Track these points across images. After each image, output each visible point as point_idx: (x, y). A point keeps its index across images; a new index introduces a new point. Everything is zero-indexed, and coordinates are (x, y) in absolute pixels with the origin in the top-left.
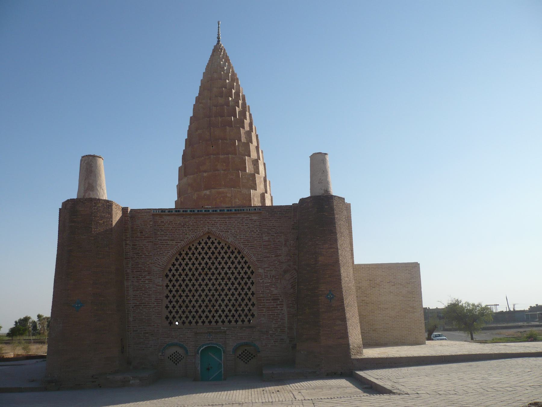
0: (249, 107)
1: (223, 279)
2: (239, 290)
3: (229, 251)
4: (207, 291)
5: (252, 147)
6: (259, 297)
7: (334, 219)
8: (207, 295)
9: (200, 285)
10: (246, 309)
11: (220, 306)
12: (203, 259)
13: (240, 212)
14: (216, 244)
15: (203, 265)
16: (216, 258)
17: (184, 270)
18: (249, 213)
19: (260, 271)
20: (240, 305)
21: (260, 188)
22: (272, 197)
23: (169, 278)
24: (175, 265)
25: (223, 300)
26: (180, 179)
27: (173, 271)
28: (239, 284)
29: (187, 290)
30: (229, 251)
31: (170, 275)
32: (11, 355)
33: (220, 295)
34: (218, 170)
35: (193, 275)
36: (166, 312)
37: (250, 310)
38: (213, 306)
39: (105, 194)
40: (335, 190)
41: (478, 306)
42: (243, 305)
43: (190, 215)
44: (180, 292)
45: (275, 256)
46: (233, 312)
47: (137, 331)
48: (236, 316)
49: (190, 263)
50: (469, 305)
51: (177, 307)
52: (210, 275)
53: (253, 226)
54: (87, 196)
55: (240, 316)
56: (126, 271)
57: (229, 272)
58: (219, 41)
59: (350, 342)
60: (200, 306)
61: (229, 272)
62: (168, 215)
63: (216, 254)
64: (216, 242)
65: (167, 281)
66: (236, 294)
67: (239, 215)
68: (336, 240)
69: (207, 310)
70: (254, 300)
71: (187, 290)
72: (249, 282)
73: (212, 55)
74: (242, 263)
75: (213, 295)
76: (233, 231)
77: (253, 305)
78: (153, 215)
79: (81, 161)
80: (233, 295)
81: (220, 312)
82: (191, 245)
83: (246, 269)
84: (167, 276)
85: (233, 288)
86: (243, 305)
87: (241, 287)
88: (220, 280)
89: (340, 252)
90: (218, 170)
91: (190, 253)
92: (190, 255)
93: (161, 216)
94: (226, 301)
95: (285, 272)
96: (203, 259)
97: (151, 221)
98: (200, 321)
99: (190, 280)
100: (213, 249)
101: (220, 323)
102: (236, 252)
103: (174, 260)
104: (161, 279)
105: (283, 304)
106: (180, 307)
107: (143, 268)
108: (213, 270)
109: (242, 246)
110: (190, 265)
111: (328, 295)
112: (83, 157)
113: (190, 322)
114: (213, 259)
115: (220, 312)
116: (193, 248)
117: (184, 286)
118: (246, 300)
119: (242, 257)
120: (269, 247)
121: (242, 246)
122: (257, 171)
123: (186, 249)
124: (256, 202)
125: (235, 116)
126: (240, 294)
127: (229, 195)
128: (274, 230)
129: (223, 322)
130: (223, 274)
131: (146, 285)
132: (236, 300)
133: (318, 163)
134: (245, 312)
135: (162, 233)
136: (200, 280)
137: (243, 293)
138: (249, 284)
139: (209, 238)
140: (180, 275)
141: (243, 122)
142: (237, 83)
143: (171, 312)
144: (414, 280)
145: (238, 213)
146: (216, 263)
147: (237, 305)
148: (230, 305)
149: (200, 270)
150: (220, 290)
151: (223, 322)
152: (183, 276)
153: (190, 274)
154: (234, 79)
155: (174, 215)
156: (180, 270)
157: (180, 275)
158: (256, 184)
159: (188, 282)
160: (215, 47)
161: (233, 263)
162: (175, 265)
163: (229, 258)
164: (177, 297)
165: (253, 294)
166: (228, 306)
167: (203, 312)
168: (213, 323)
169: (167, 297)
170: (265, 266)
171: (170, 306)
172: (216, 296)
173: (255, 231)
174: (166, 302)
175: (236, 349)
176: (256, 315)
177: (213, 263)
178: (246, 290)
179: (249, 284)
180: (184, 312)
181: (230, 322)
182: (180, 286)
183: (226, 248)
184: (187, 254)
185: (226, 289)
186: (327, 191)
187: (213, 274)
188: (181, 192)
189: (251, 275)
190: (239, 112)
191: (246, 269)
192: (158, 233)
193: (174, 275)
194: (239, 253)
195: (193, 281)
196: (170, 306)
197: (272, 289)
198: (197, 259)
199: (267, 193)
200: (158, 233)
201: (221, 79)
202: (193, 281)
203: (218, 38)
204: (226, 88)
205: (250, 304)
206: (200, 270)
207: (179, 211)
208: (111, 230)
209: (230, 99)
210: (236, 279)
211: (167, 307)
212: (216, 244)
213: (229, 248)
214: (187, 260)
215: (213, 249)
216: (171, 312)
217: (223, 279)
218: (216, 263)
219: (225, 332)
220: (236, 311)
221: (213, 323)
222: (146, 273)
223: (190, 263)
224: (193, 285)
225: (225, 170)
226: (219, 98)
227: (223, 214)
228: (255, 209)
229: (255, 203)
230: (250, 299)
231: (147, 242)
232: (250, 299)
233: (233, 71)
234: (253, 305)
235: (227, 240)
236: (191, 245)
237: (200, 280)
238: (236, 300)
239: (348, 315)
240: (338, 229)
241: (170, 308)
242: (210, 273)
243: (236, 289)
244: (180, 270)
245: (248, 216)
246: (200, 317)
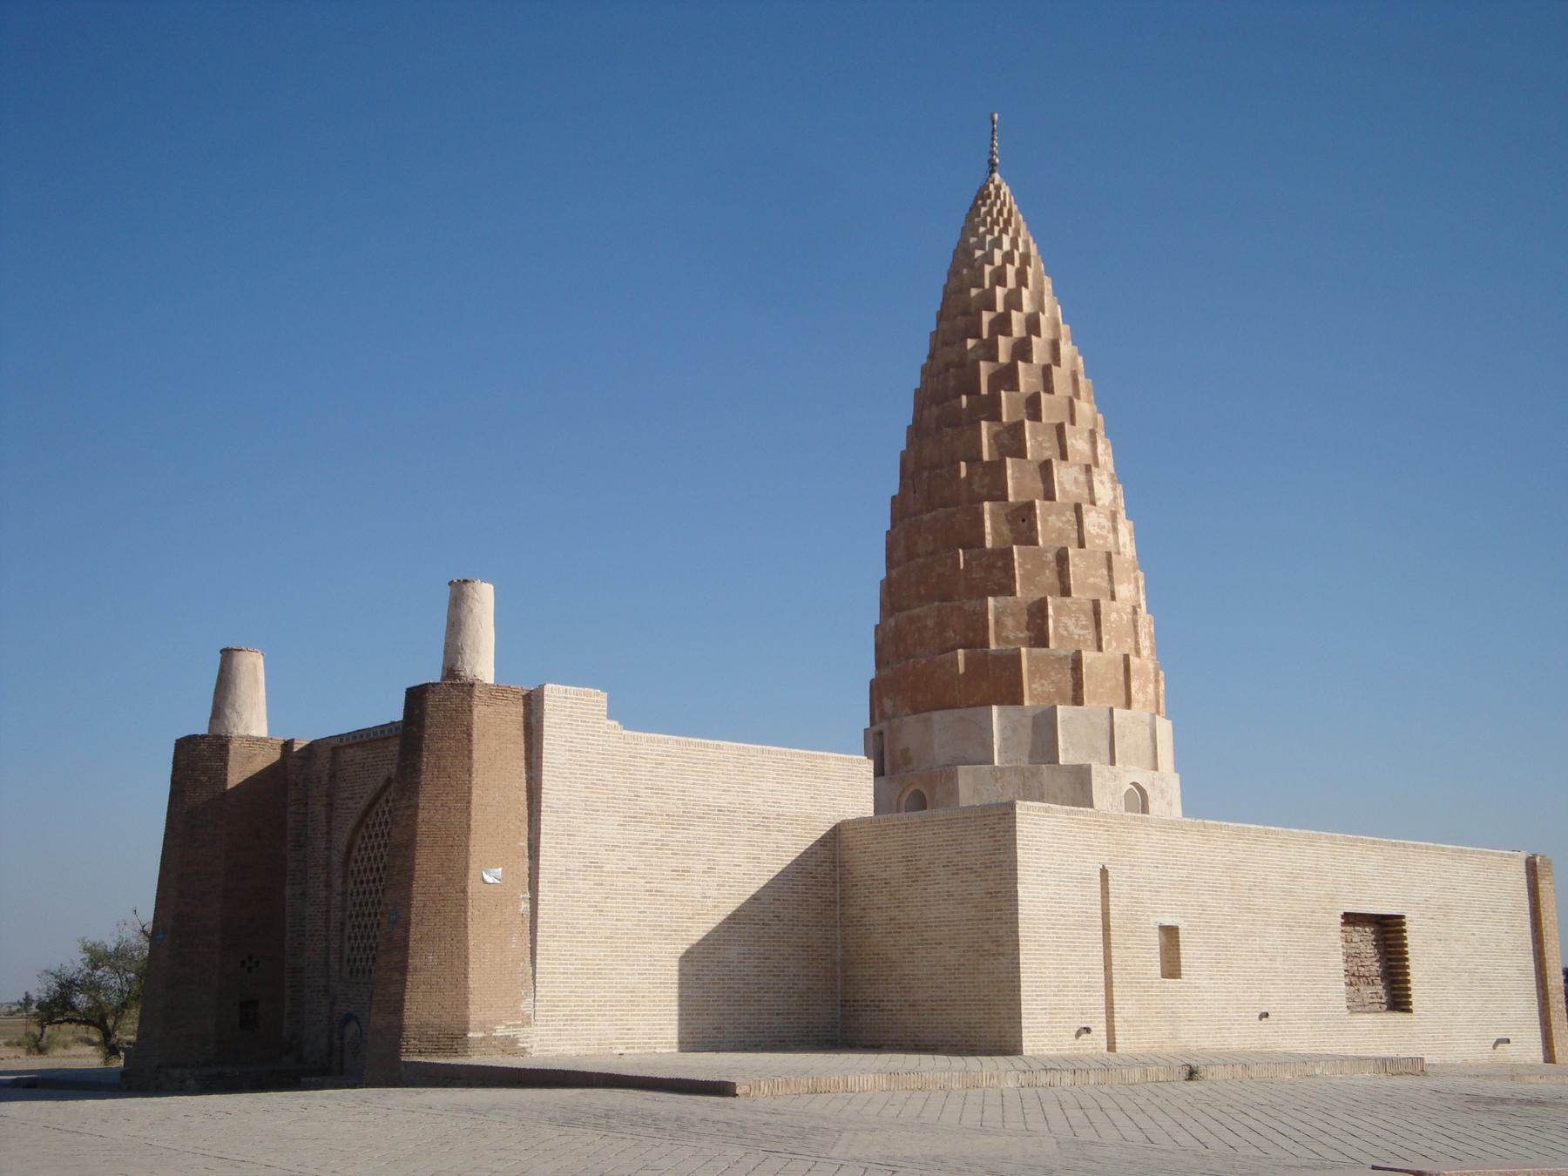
7: (421, 739)
34: (918, 556)
54: (217, 732)
59: (406, 1022)
62: (350, 746)
78: (335, 749)
89: (422, 815)
125: (973, 390)
127: (930, 623)
144: (1002, 857)
190: (991, 378)
199: (1066, 591)
203: (992, 164)
208: (226, 793)
239: (413, 962)
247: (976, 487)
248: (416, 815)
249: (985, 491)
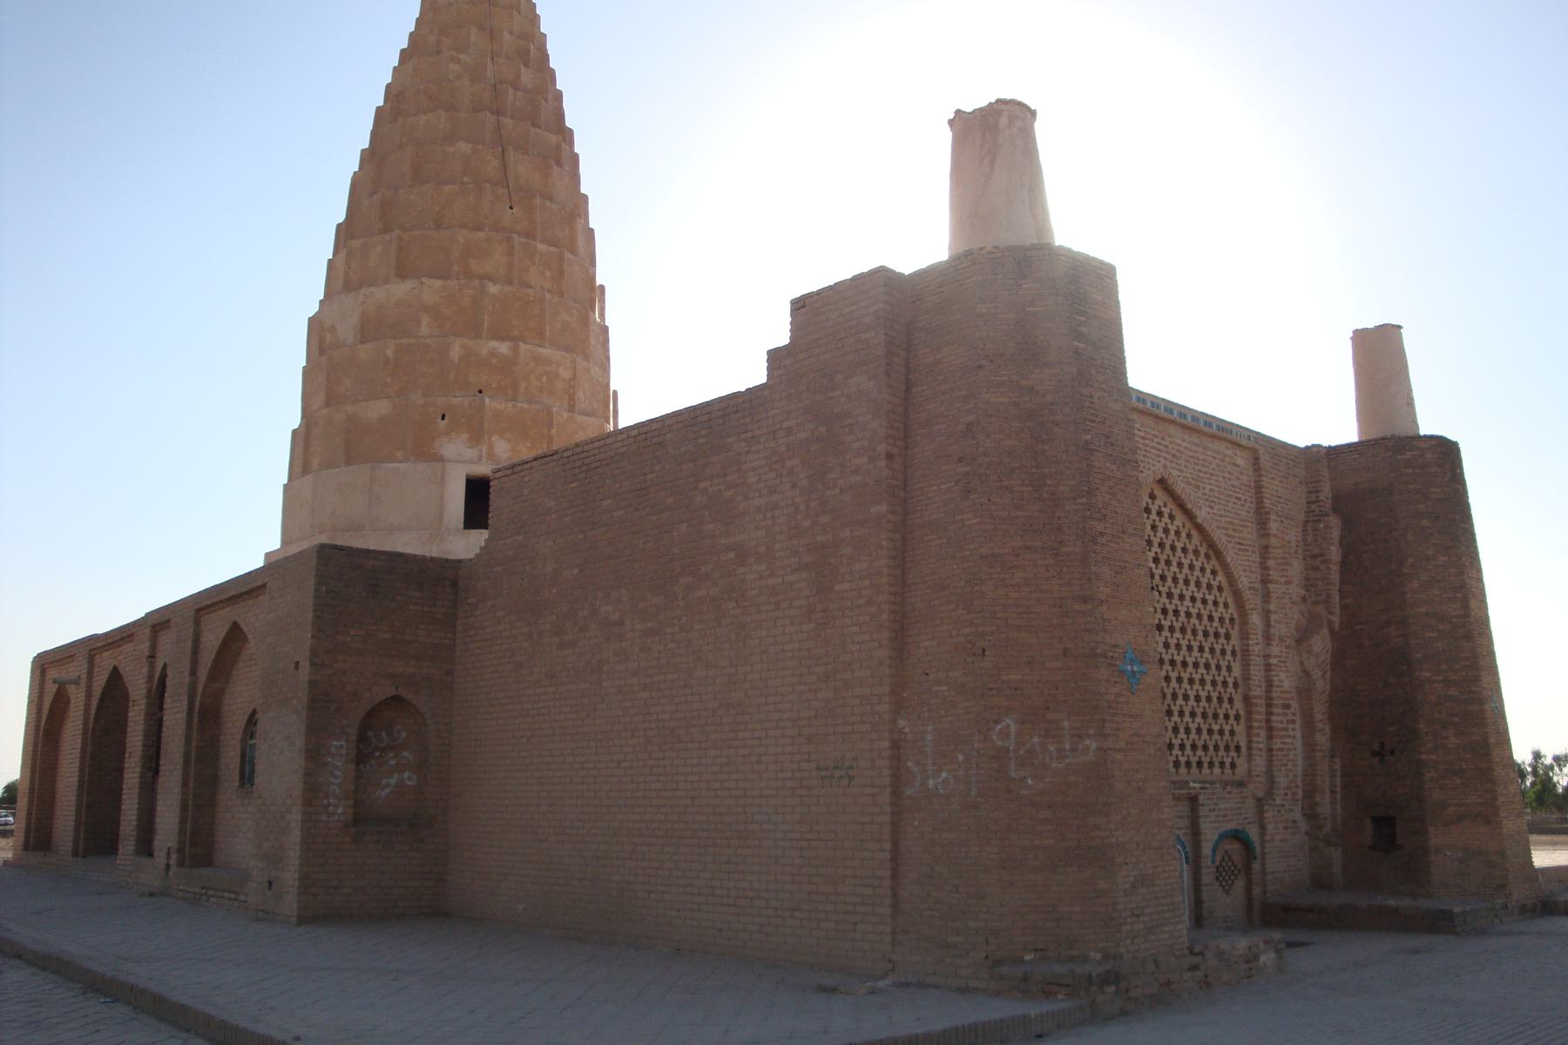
67: (1216, 445)
105: (1293, 722)
121: (1224, 539)
127: (565, 374)
197: (1283, 676)
235: (1198, 513)
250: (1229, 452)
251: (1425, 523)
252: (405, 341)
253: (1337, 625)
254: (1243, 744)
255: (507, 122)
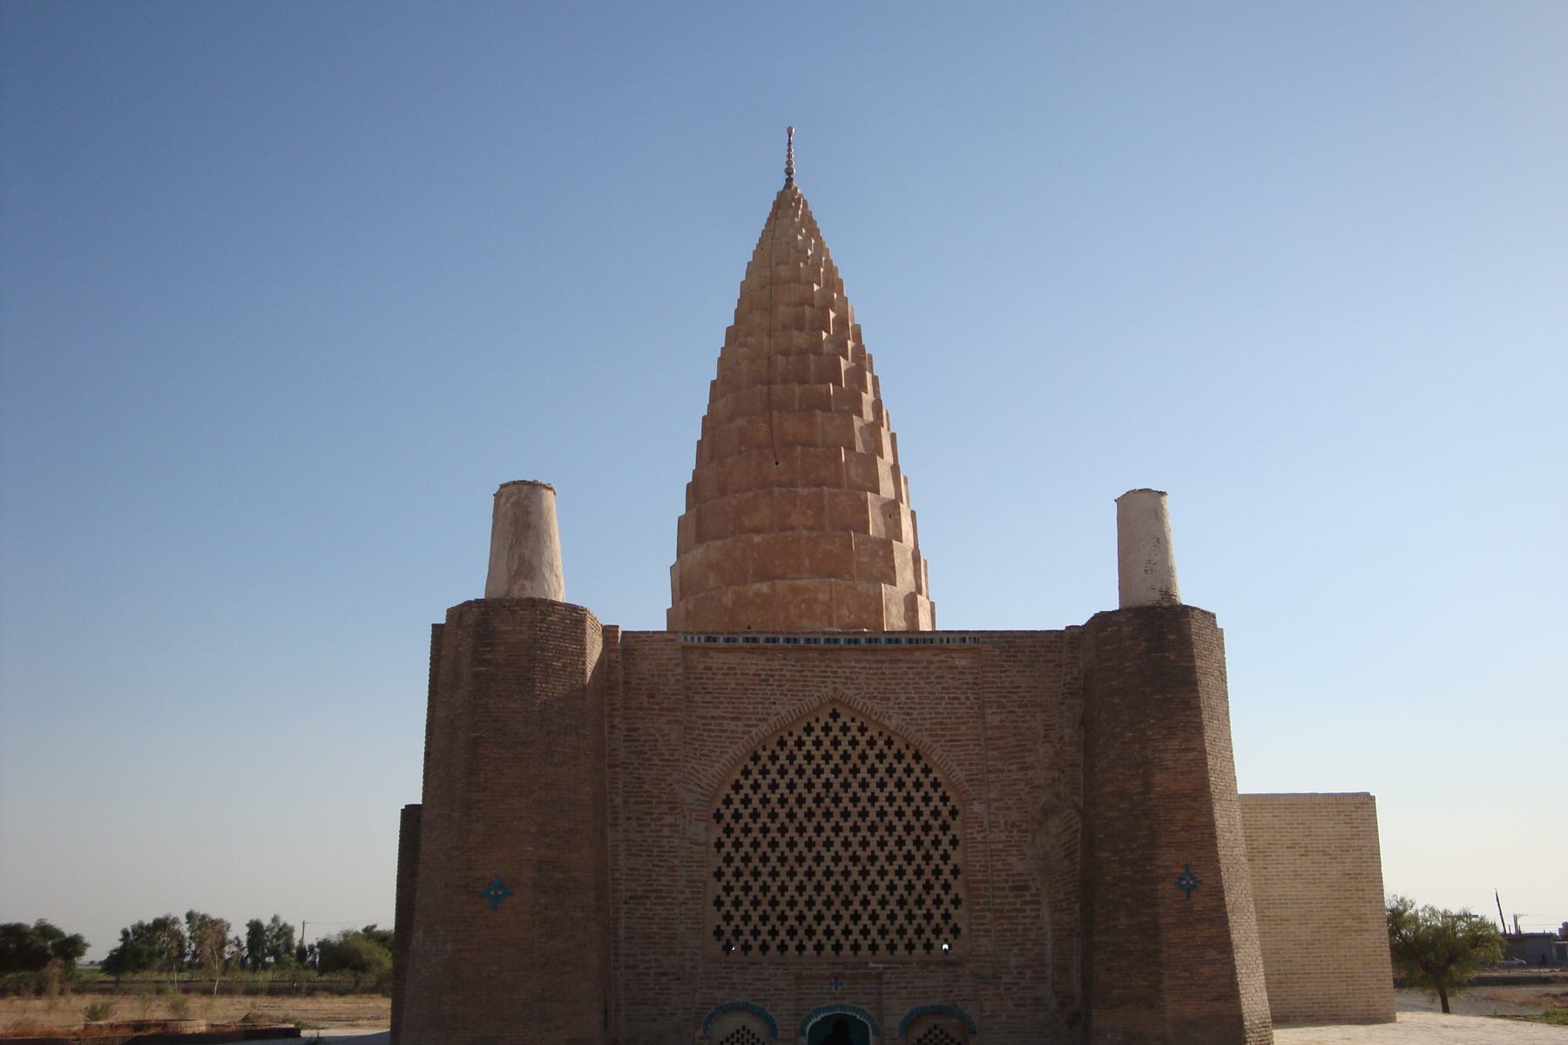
0: (870, 357)
1: (873, 829)
2: (919, 859)
3: (890, 753)
4: (828, 861)
5: (884, 465)
6: (975, 882)
7: (1192, 670)
8: (828, 874)
9: (810, 844)
10: (937, 914)
11: (865, 902)
12: (818, 771)
13: (921, 645)
14: (854, 732)
15: (819, 788)
16: (855, 771)
17: (765, 801)
18: (944, 650)
19: (977, 807)
20: (920, 902)
21: (905, 576)
22: (932, 604)
23: (723, 824)
24: (741, 787)
25: (873, 888)
26: (682, 550)
27: (737, 804)
28: (918, 843)
29: (773, 857)
30: (890, 753)
31: (728, 814)
32: (199, 1026)
33: (864, 873)
34: (792, 528)
35: (791, 816)
36: (716, 918)
37: (946, 916)
38: (847, 903)
39: (563, 588)
40: (1186, 595)
41: (1459, 918)
42: (929, 902)
43: (784, 650)
44: (755, 862)
45: (1020, 769)
46: (901, 920)
47: (635, 967)
48: (911, 932)
49: (783, 783)
50: (1433, 912)
51: (746, 905)
52: (837, 818)
53: (957, 683)
54: (516, 594)
55: (919, 931)
56: (612, 800)
57: (891, 810)
58: (789, 181)
59: (1245, 1009)
60: (810, 903)
61: (891, 810)
62: (725, 650)
63: (855, 759)
64: (854, 726)
65: (718, 832)
66: (910, 870)
68: (1199, 729)
69: (828, 915)
70: (957, 887)
71: (773, 857)
72: (945, 840)
73: (773, 217)
74: (927, 787)
75: (846, 874)
76: (903, 698)
77: (956, 902)
78: (684, 648)
79: (498, 496)
80: (900, 873)
81: (865, 920)
82: (785, 735)
83: (936, 802)
84: (718, 816)
85: (900, 855)
86: (929, 902)
87: (923, 852)
88: (864, 832)
89: (1210, 762)
90: (792, 528)
91: (783, 756)
92: (783, 760)
93: (705, 651)
94: (882, 891)
95: (1048, 812)
96: (818, 771)
97: (677, 665)
98: (809, 945)
99: (783, 830)
100: (845, 746)
101: (865, 952)
102: (909, 755)
103: (737, 775)
104: (703, 825)
105: (1039, 903)
106: (756, 903)
107: (656, 792)
108: (846, 803)
109: (927, 740)
110: (783, 789)
111: (1181, 879)
112: (503, 486)
113: (783, 947)
114: (845, 773)
115: (865, 920)
116: (791, 743)
117: (764, 847)
118: (937, 890)
119: (926, 771)
120: (1001, 742)
121: (927, 740)
122: (895, 532)
123: (773, 745)
124: (894, 620)
125: (837, 383)
126: (919, 872)
127: (822, 597)
128: (1015, 697)
129: (873, 947)
130: (873, 816)
131: (665, 842)
132: (910, 887)
133: (1141, 520)
134: (933, 923)
135: (708, 698)
136: (810, 832)
137: (928, 869)
138: (945, 844)
139: (835, 715)
140: (755, 816)
141: (859, 400)
142: (840, 293)
143: (728, 918)
144: (1361, 843)
145: (917, 649)
146: (855, 786)
147: (911, 900)
148: (893, 900)
149: (810, 803)
150: (864, 861)
151: (873, 947)
152: (764, 818)
153: (782, 813)
154: (833, 283)
155: (741, 648)
156: (755, 802)
157: (755, 816)
158: (893, 568)
159: (777, 836)
160: (781, 195)
161: (900, 785)
162: (741, 787)
163: (891, 770)
164: (747, 877)
165: (955, 872)
166: (887, 903)
167: (819, 918)
168: (846, 951)
169: (719, 874)
170: (992, 796)
171: (728, 901)
172: (855, 876)
173: (963, 698)
174: (717, 888)
175: (908, 1025)
176: (964, 931)
177: (846, 785)
178: (936, 860)
179: (945, 844)
180: (764, 918)
181: (892, 947)
182: (755, 844)
183: (881, 743)
184: (774, 758)
185: (882, 855)
186: (1168, 594)
187: (846, 815)
188: (684, 583)
189: (950, 820)
191: (936, 802)
192: (698, 698)
193: (737, 816)
194: (917, 757)
195: (792, 832)
196: (728, 901)
197: (1012, 860)
198: (800, 772)
200: (698, 698)
201: (797, 281)
202: (792, 832)
203: (789, 172)
204: (812, 305)
205: (947, 899)
206: (810, 803)
207: (755, 640)
208: (584, 689)
209: (824, 335)
210: (909, 828)
211: (719, 903)
212: (854, 732)
213: (889, 743)
214: (774, 775)
215: (845, 746)
216: (728, 918)
217: (873, 829)
218: (855, 786)
219: (879, 976)
220: (910, 917)
221: (846, 951)
222: (665, 808)
223: (783, 783)
224: (792, 844)
225: (811, 529)
226: (795, 332)
227: (874, 651)
228: (964, 640)
229: (893, 620)
230: (946, 887)
231: (668, 723)
232: (946, 887)
233: (829, 262)
234: (956, 902)
235: (886, 722)
236: (785, 735)
237: (810, 832)
238: (910, 887)
239: (1235, 936)
240: (1203, 697)
241: (728, 906)
242: (836, 812)
243: (909, 858)
244: (755, 802)
245: (942, 657)
246: (810, 933)
247: (852, 473)
248: (1204, 761)
249: (859, 481)
250: (942, 657)
251: (1117, 700)
252: (700, 595)
253: (1081, 804)
254: (962, 925)
255: (777, 388)
